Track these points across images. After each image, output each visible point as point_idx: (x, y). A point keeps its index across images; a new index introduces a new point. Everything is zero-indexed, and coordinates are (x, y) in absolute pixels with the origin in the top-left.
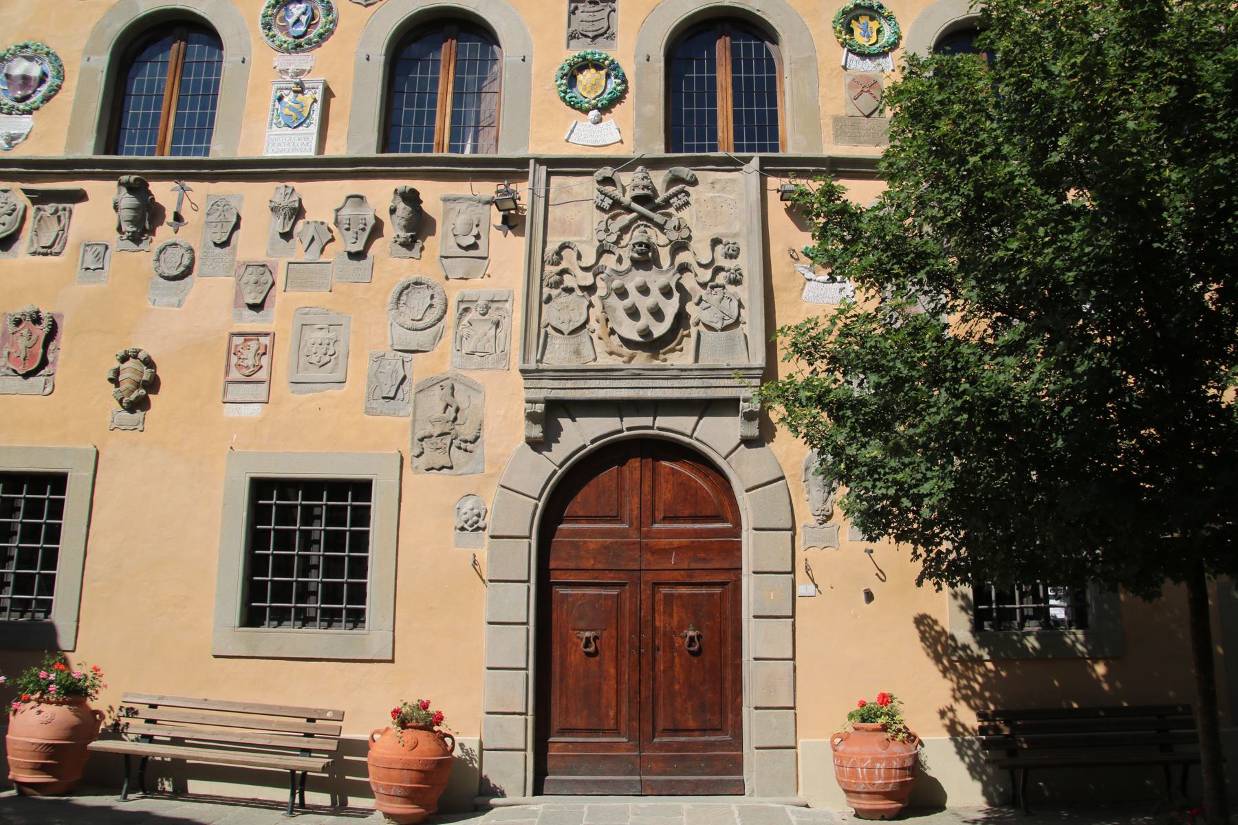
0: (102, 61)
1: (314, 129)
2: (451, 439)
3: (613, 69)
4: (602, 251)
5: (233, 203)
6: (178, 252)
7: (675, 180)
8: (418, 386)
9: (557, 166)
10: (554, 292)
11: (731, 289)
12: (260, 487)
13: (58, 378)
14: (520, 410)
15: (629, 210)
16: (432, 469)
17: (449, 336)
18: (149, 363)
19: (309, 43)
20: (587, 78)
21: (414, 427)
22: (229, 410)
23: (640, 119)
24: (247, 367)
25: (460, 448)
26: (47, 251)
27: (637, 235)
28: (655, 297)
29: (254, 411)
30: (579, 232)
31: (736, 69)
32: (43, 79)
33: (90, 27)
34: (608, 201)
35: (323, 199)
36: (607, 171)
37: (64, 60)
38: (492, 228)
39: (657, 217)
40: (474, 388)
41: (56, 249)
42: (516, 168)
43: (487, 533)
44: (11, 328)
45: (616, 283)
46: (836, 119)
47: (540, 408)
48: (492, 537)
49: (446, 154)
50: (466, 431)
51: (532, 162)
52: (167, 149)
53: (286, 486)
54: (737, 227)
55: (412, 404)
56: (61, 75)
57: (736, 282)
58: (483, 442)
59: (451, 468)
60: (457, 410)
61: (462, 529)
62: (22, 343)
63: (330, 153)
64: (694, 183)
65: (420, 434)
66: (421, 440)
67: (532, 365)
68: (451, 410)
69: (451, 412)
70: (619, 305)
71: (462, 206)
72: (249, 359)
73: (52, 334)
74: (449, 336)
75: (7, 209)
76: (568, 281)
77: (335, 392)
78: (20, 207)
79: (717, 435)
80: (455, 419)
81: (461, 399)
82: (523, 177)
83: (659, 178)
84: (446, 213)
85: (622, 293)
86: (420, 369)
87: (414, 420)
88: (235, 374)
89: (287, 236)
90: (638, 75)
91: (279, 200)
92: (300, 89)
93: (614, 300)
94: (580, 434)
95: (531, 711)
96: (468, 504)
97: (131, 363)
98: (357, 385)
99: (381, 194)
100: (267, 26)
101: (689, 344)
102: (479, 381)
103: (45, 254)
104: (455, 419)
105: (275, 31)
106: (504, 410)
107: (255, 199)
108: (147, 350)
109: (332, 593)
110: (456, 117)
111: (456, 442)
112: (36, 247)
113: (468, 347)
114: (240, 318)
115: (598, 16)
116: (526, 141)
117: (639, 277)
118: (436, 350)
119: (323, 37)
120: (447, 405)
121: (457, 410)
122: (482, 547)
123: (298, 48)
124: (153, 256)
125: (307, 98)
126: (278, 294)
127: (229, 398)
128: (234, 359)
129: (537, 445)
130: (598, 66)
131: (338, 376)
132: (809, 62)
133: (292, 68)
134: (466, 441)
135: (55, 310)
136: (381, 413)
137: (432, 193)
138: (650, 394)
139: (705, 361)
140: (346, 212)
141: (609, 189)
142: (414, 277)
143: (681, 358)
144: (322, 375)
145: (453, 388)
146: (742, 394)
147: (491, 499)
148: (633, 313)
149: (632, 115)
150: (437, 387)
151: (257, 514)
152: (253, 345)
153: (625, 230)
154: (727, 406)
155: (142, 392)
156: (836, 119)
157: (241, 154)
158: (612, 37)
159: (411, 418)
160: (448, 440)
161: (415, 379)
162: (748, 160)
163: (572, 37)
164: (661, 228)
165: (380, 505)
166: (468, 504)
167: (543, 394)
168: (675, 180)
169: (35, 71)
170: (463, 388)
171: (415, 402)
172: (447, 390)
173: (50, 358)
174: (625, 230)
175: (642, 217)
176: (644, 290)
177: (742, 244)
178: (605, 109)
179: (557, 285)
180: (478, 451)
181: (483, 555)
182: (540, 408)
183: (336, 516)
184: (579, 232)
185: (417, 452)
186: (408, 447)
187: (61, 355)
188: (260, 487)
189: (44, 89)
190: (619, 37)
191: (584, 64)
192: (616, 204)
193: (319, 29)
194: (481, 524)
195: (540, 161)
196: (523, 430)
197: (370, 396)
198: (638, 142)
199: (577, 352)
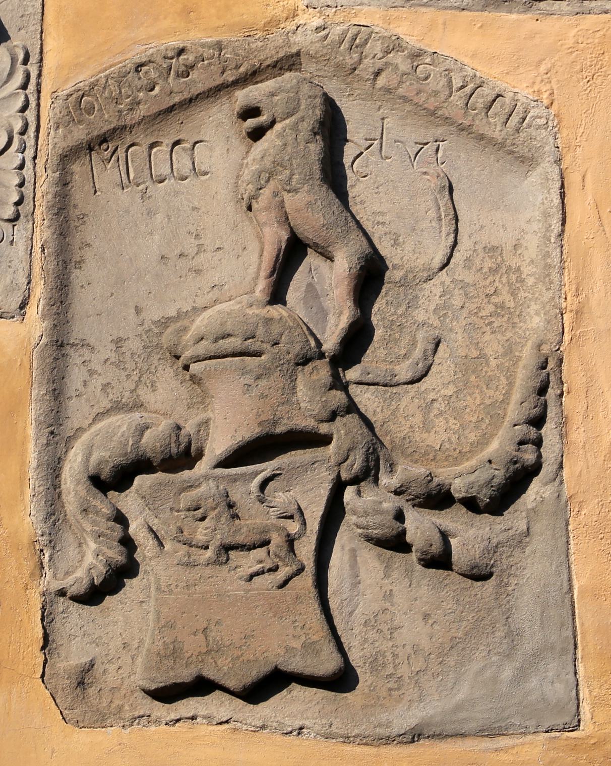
8: (79, 104)
16: (202, 686)
21: (57, 394)
40: (483, 126)
50: (446, 425)
55: (43, 233)
58: (561, 509)
59: (342, 680)
60: (370, 277)
65: (100, 440)
66: (114, 480)
68: (328, 281)
69: (325, 293)
80: (358, 338)
87: (59, 344)
102: (520, 87)
104: (358, 338)
111: (366, 505)
120: (294, 252)
121: (370, 277)
134: (438, 499)
145: (332, 127)
150: (217, 124)
159: (35, 323)
160: (305, 486)
170: (401, 130)
171: (62, 207)
172: (291, 141)
180: (531, 571)
185: (89, 559)
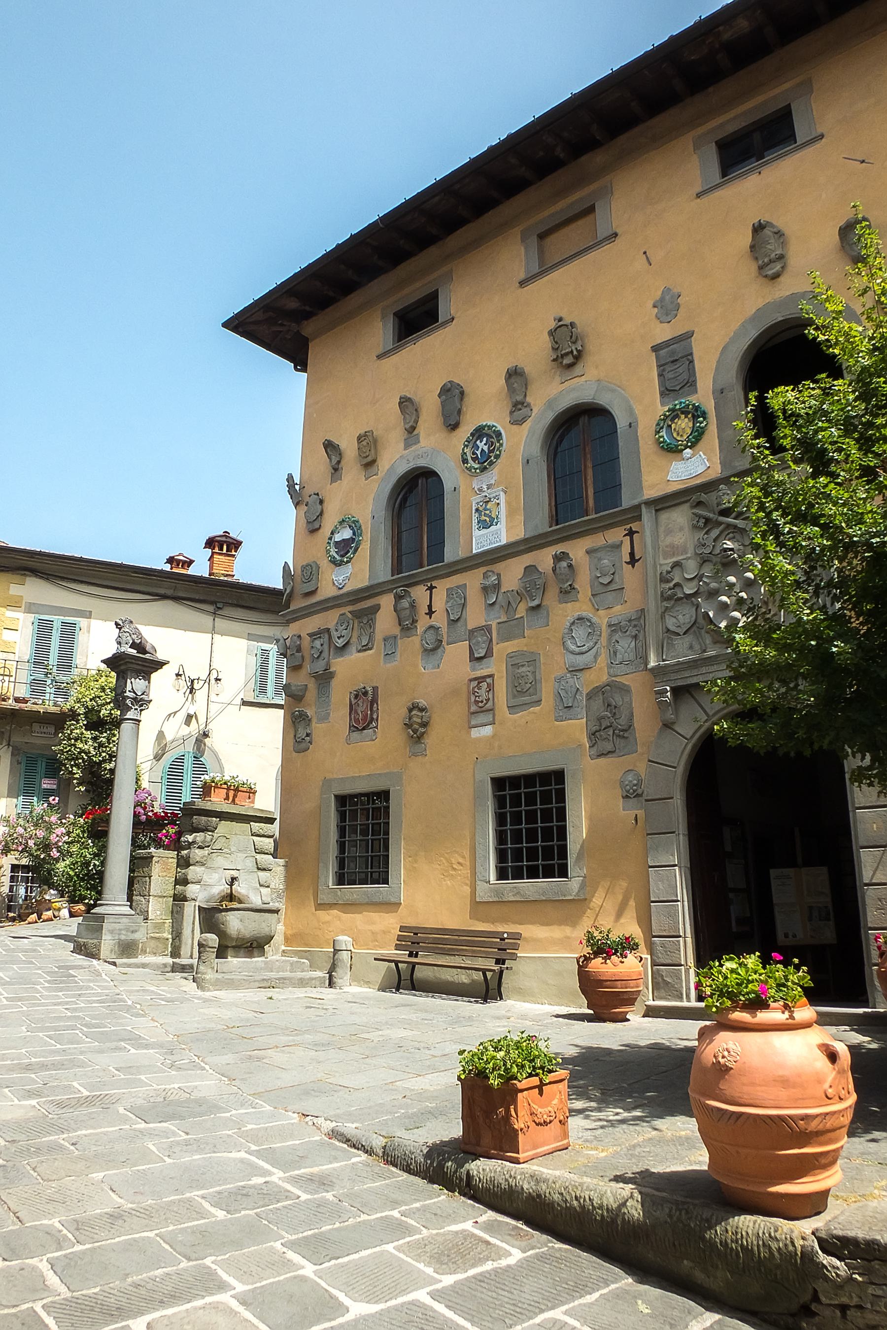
9: (663, 503)
12: (499, 783)
22: (475, 733)
24: (482, 702)
25: (619, 736)
26: (366, 648)
29: (488, 731)
38: (624, 564)
41: (370, 645)
43: (642, 799)
48: (647, 800)
50: (623, 721)
51: (643, 506)
52: (426, 562)
61: (627, 797)
66: (593, 734)
73: (374, 701)
81: (617, 699)
88: (474, 708)
100: (465, 461)
103: (365, 650)
112: (359, 648)
115: (680, 370)
131: (535, 698)
136: (566, 719)
142: (576, 615)
144: (526, 699)
151: (500, 802)
152: (484, 685)
169: (347, 534)
184: (685, 551)
188: (499, 783)
192: (707, 520)
194: (640, 791)
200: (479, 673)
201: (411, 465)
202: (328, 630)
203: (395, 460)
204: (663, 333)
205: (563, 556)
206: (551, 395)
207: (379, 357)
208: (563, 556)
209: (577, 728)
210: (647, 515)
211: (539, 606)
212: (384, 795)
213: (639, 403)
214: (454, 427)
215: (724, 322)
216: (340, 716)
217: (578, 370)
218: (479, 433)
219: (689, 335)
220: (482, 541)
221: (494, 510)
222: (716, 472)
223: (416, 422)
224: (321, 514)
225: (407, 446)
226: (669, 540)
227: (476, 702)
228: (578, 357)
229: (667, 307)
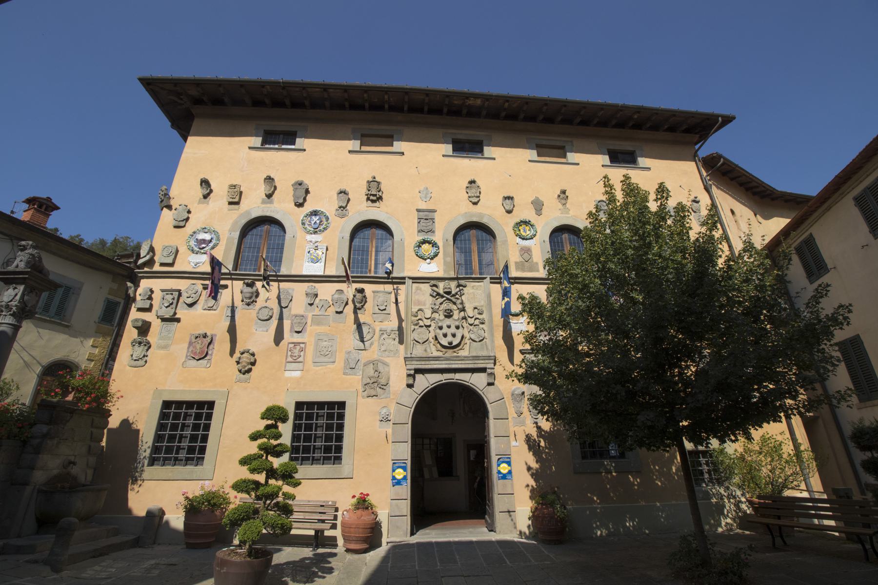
0: (236, 235)
1: (323, 264)
2: (376, 385)
3: (434, 245)
4: (434, 311)
5: (290, 291)
6: (267, 310)
7: (459, 286)
9: (416, 280)
10: (416, 327)
11: (481, 326)
13: (213, 360)
14: (404, 373)
15: (443, 297)
17: (376, 344)
18: (253, 355)
19: (320, 231)
20: (426, 246)
23: (445, 263)
26: (210, 308)
27: (445, 306)
28: (453, 330)
29: (297, 374)
30: (424, 305)
31: (478, 244)
32: (210, 241)
33: (231, 221)
34: (435, 294)
35: (326, 291)
36: (433, 282)
37: (220, 234)
39: (453, 299)
40: (385, 364)
41: (215, 307)
42: (401, 281)
43: (391, 423)
44: (194, 340)
45: (440, 324)
46: (516, 263)
47: (412, 372)
49: (372, 275)
50: (383, 381)
53: (310, 405)
54: (482, 303)
56: (218, 239)
57: (483, 323)
62: (198, 346)
63: (328, 273)
64: (465, 287)
67: (409, 356)
70: (440, 333)
71: (381, 295)
72: (296, 352)
74: (376, 344)
75: (194, 291)
76: (421, 323)
77: (331, 366)
78: (200, 291)
79: (477, 381)
81: (381, 368)
82: (404, 283)
83: (453, 285)
84: (374, 297)
85: (441, 328)
86: (365, 356)
88: (290, 359)
89: (311, 305)
90: (444, 246)
91: (309, 291)
92: (316, 248)
93: (438, 331)
94: (425, 383)
95: (409, 498)
96: (384, 410)
97: (245, 355)
98: (340, 363)
99: (349, 290)
100: (303, 224)
101: (467, 347)
105: (306, 226)
106: (397, 374)
107: (299, 290)
108: (253, 349)
109: (328, 449)
110: (376, 260)
112: (206, 307)
113: (383, 348)
114: (292, 336)
116: (403, 271)
117: (448, 322)
118: (371, 350)
119: (325, 229)
122: (389, 429)
123: (315, 233)
124: (256, 311)
125: (319, 252)
126: (309, 328)
127: (287, 368)
128: (289, 353)
129: (410, 386)
130: (429, 243)
131: (331, 360)
132: (505, 242)
133: (314, 240)
135: (213, 333)
137: (369, 288)
138: (454, 366)
139: (474, 354)
140: (336, 296)
141: (435, 288)
143: (464, 353)
144: (326, 359)
146: (488, 366)
147: (393, 408)
148: (445, 335)
149: (442, 261)
152: (298, 348)
153: (441, 304)
154: (483, 370)
155: (250, 366)
156: (516, 263)
157: (294, 272)
158: (434, 232)
161: (363, 361)
162: (485, 278)
163: (419, 231)
164: (455, 303)
165: (348, 412)
166: (384, 410)
167: (413, 367)
168: (459, 286)
169: (207, 237)
173: (210, 352)
174: (441, 304)
175: (448, 299)
176: (449, 327)
177: (484, 309)
178: (432, 259)
179: (416, 325)
181: (390, 431)
182: (412, 372)
183: (330, 416)
184: (424, 305)
186: (360, 388)
187: (215, 351)
189: (211, 245)
190: (436, 232)
191: (424, 242)
192: (438, 294)
193: (324, 226)
195: (410, 278)
196: (404, 381)
197: (345, 368)
198: (445, 271)
199: (426, 350)
200: (295, 340)
201: (268, 214)
202: (179, 291)
203: (254, 206)
204: (423, 206)
205: (361, 291)
206: (361, 211)
207: (250, 148)
208: (361, 291)
209: (356, 381)
210: (409, 282)
211: (341, 312)
212: (211, 405)
213: (406, 232)
214: (300, 205)
215: (453, 212)
216: (181, 349)
217: (377, 204)
218: (315, 213)
219: (434, 211)
220: (310, 269)
221: (312, 252)
222: (441, 274)
223: (273, 192)
224: (187, 219)
225: (263, 202)
226: (417, 297)
227: (291, 356)
228: (380, 198)
229: (426, 194)
